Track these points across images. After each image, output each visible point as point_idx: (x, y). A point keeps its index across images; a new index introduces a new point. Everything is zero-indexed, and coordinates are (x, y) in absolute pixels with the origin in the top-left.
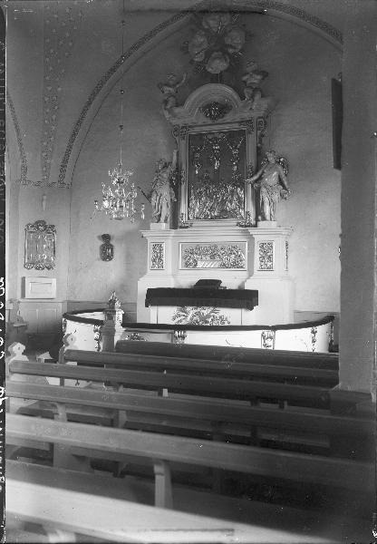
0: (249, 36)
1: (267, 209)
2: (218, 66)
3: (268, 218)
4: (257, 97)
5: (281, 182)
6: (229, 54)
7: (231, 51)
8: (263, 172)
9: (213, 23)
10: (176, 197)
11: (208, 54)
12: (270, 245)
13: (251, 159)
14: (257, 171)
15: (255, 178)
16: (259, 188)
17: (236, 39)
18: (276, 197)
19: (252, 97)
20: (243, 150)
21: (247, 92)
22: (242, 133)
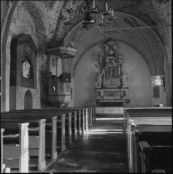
0: (118, 47)
1: (124, 84)
2: (111, 53)
3: (124, 85)
4: (121, 61)
5: (126, 78)
6: (114, 50)
7: (114, 50)
8: (123, 76)
9: (110, 43)
10: (102, 80)
11: (109, 50)
12: (125, 91)
13: (120, 73)
14: (121, 75)
15: (121, 77)
16: (122, 79)
17: (115, 47)
18: (125, 81)
19: (120, 60)
20: (117, 71)
21: (119, 59)
22: (117, 67)
